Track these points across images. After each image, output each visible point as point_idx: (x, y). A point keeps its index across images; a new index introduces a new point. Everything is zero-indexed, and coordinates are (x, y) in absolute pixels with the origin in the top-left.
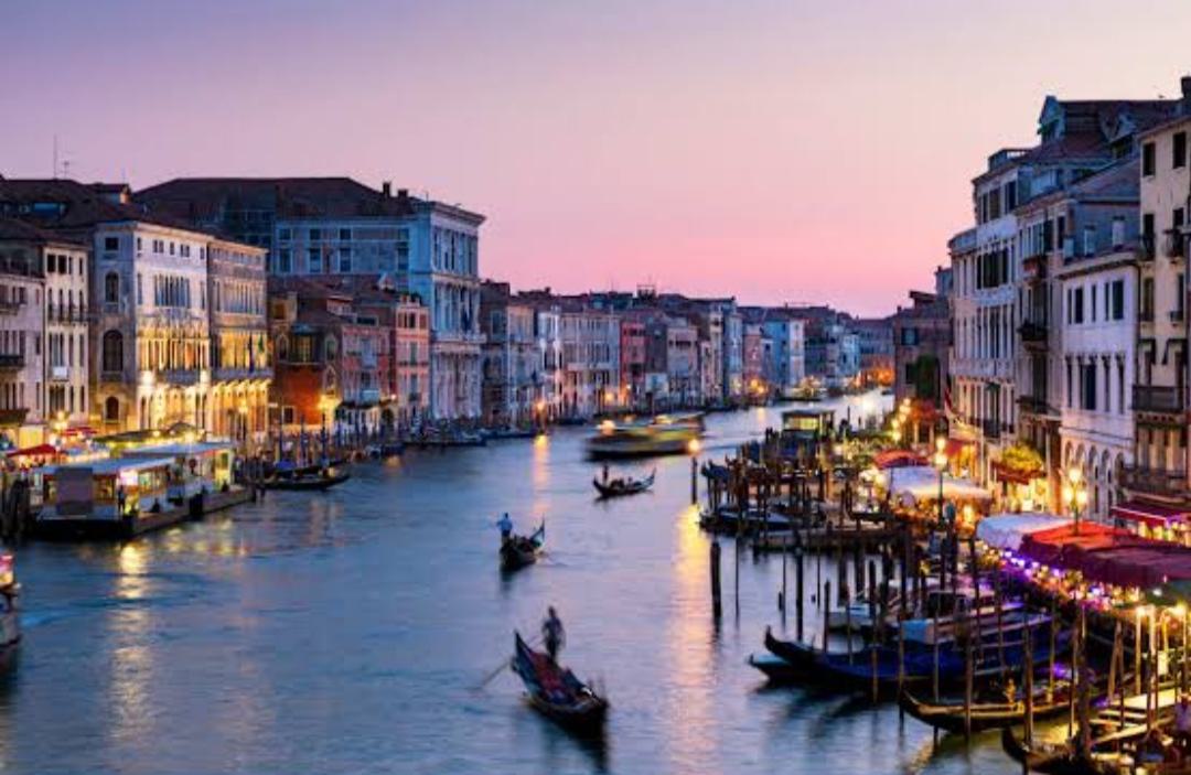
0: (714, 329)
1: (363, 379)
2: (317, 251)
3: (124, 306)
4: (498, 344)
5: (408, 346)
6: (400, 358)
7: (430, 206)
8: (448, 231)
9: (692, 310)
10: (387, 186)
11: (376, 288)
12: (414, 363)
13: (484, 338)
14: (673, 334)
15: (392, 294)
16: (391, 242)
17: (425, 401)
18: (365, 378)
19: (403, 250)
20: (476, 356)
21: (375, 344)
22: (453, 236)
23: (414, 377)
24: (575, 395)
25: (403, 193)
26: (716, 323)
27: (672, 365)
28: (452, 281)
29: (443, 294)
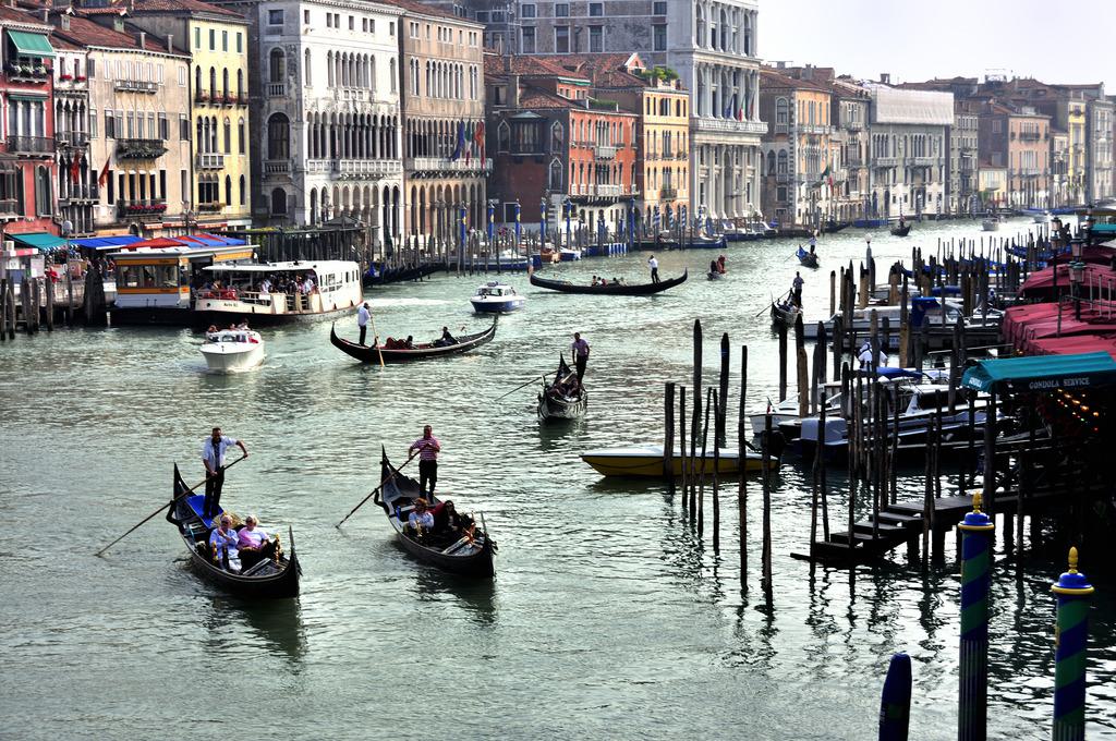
0: (1072, 119)
2: (566, 28)
3: (290, 87)
4: (783, 135)
5: (659, 136)
6: (648, 148)
9: (1049, 101)
11: (623, 69)
12: (667, 155)
13: (764, 128)
14: (1016, 125)
17: (682, 197)
18: (602, 172)
19: (661, 27)
20: (754, 147)
23: (667, 171)
24: (887, 195)
26: (1077, 113)
27: (1014, 163)
28: (721, 61)
29: (708, 78)
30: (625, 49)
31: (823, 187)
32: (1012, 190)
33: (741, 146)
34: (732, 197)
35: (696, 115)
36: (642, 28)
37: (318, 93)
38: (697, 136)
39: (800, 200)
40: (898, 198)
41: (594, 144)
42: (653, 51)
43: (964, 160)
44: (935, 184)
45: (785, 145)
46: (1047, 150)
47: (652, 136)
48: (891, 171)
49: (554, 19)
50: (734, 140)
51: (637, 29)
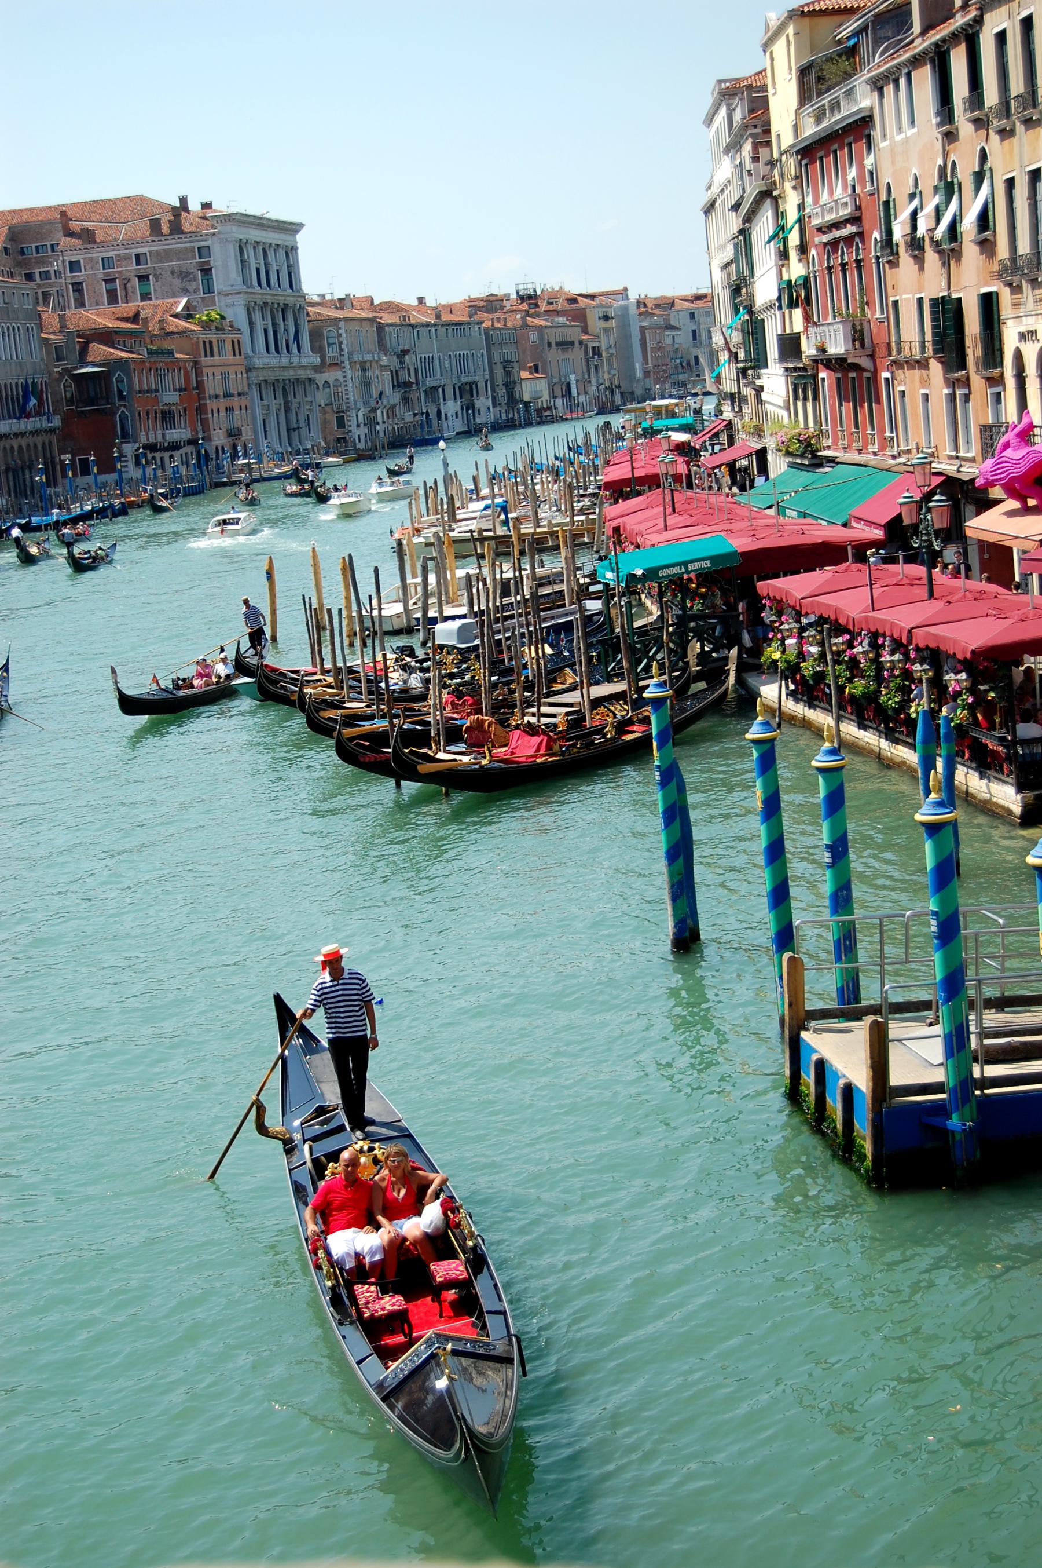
1: (163, 418)
2: (113, 280)
4: (337, 364)
5: (218, 377)
8: (258, 242)
10: (183, 200)
12: (227, 395)
16: (192, 263)
17: (247, 435)
18: (167, 417)
19: (206, 271)
21: (176, 378)
23: (230, 409)
24: (439, 412)
25: (207, 206)
29: (257, 317)
30: (174, 295)
31: (379, 412)
32: (555, 397)
33: (297, 380)
34: (294, 430)
35: (251, 354)
36: (188, 274)
38: (254, 374)
39: (358, 426)
40: (449, 415)
41: (157, 391)
42: (202, 295)
43: (508, 373)
44: (483, 398)
45: (338, 374)
46: (582, 356)
47: (211, 377)
48: (440, 390)
49: (101, 272)
50: (290, 374)
51: (184, 275)
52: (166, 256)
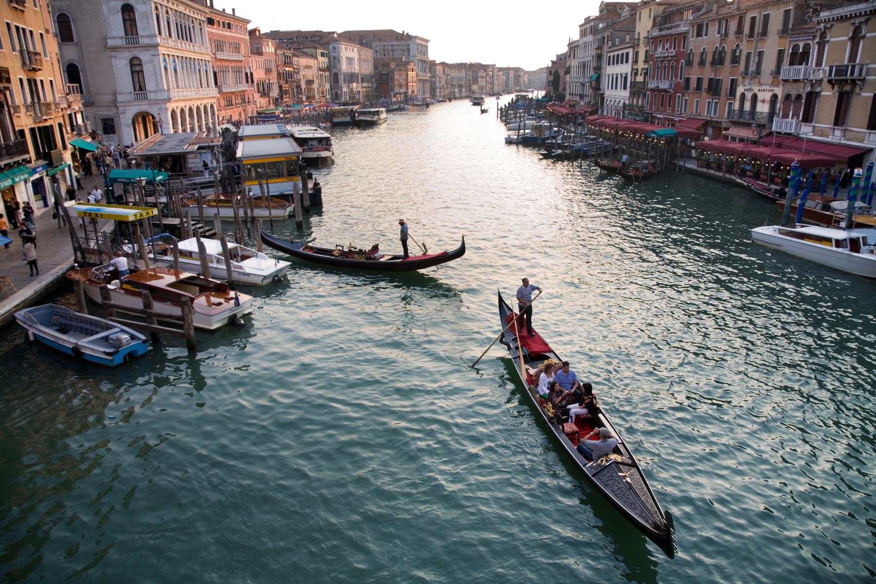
7: (416, 37)
9: (485, 67)
14: (480, 74)
15: (408, 63)
18: (400, 86)
19: (409, 50)
22: (422, 46)
27: (480, 83)
37: (344, 67)
51: (403, 51)
52: (399, 45)
